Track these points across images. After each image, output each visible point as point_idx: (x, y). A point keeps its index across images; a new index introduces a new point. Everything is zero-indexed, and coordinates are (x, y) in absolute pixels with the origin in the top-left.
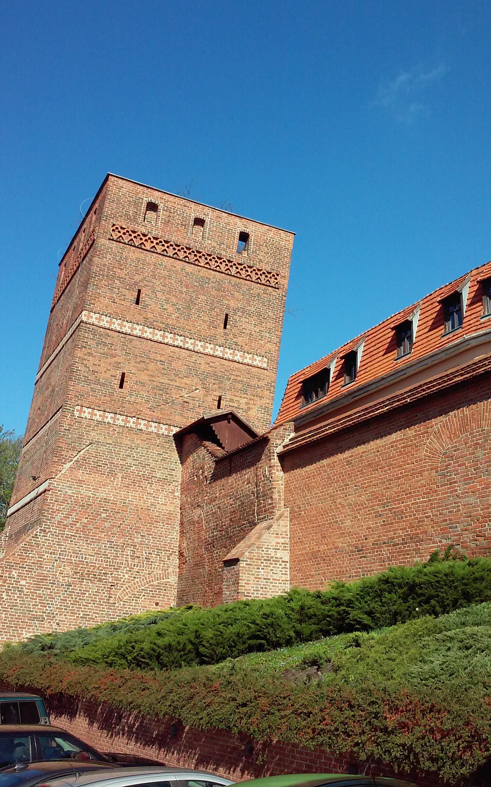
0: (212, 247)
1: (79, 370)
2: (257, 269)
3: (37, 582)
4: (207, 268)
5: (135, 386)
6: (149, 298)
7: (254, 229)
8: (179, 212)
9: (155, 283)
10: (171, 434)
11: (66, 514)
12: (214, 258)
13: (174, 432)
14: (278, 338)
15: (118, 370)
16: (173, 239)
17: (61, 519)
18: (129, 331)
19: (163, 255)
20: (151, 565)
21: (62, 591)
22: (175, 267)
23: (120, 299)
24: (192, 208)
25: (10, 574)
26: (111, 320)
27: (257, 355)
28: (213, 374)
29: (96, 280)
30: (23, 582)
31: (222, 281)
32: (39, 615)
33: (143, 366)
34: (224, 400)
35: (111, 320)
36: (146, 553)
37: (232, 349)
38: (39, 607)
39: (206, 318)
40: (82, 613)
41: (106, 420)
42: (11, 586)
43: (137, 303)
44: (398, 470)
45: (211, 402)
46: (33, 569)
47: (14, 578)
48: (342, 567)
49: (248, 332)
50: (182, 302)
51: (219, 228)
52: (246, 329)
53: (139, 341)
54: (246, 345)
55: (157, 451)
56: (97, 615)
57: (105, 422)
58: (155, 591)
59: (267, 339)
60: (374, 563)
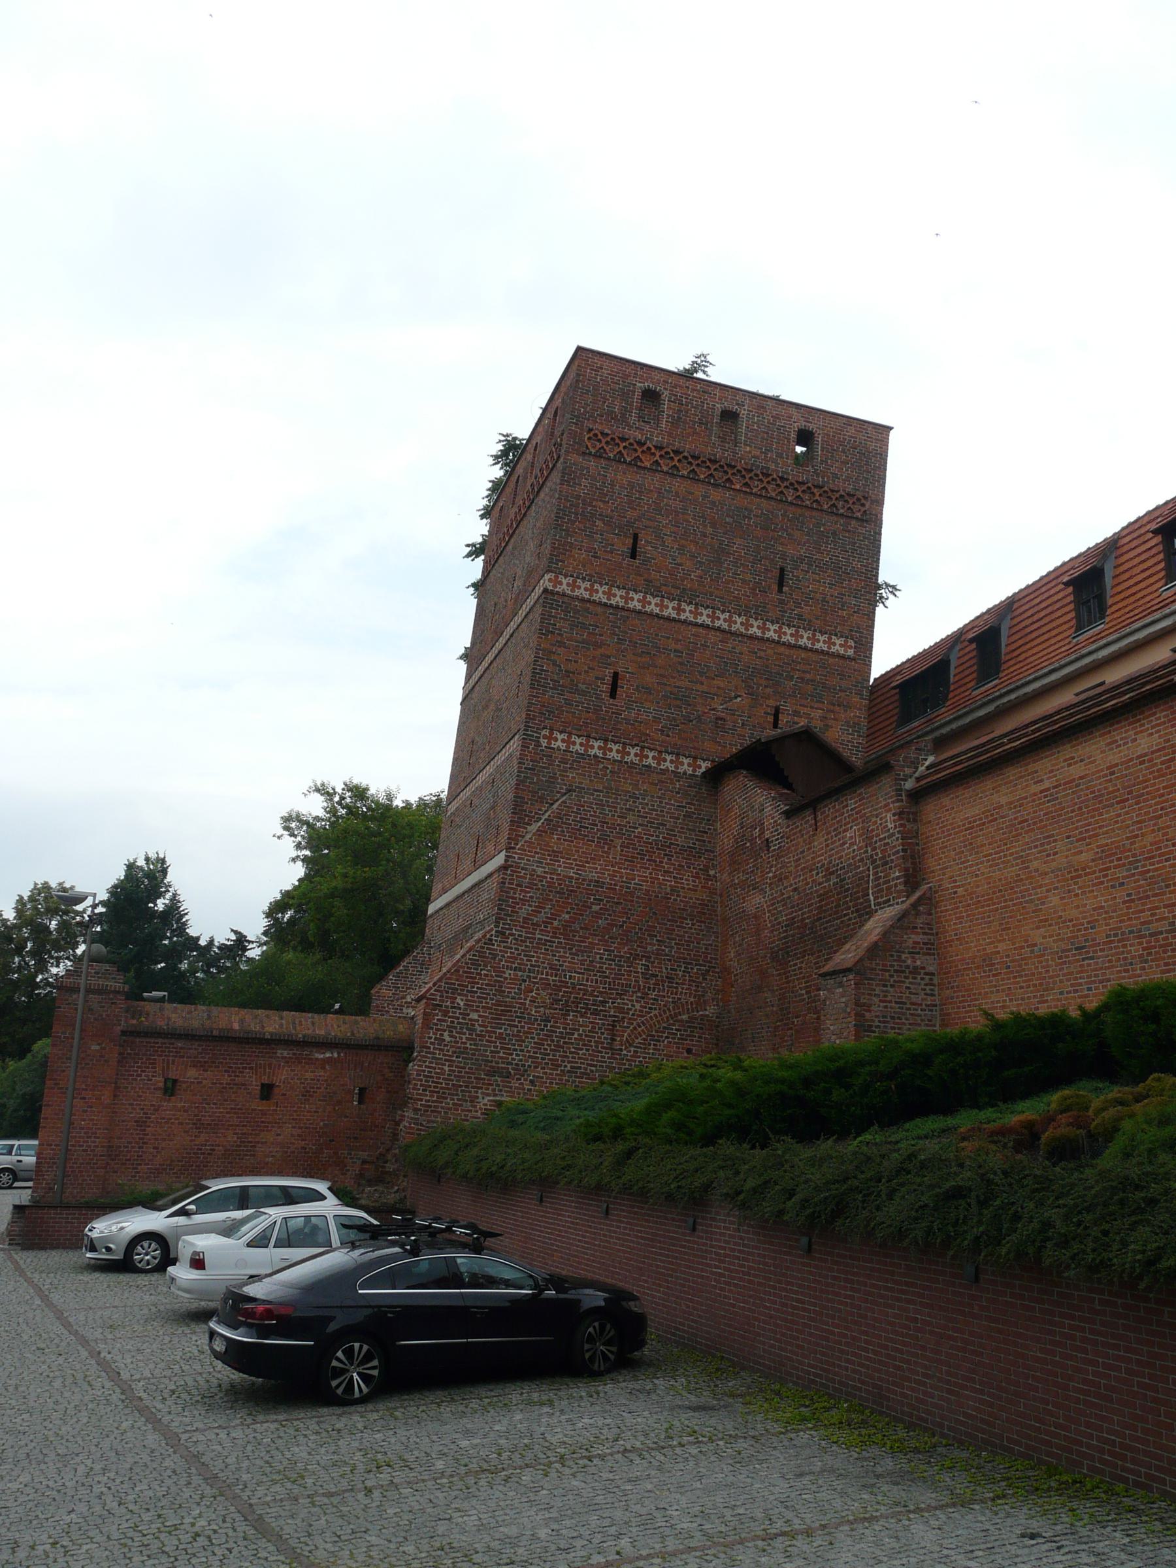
1: (545, 671)
3: (496, 1014)
4: (746, 492)
10: (699, 772)
11: (536, 907)
12: (757, 475)
13: (703, 770)
16: (688, 447)
17: (528, 914)
18: (621, 603)
19: (672, 475)
20: (676, 988)
21: (536, 1029)
22: (693, 493)
23: (606, 551)
25: (452, 1003)
26: (592, 586)
27: (836, 635)
30: (474, 1016)
31: (772, 513)
32: (502, 1068)
35: (592, 586)
36: (667, 969)
37: (794, 626)
38: (501, 1055)
39: (749, 577)
40: (569, 1065)
41: (592, 752)
42: (456, 1021)
43: (633, 555)
44: (1156, 804)
45: (762, 717)
46: (489, 994)
47: (460, 1009)
48: (1044, 978)
54: (817, 619)
55: (675, 801)
56: (593, 1068)
57: (590, 756)
58: (685, 1031)
60: (1112, 967)
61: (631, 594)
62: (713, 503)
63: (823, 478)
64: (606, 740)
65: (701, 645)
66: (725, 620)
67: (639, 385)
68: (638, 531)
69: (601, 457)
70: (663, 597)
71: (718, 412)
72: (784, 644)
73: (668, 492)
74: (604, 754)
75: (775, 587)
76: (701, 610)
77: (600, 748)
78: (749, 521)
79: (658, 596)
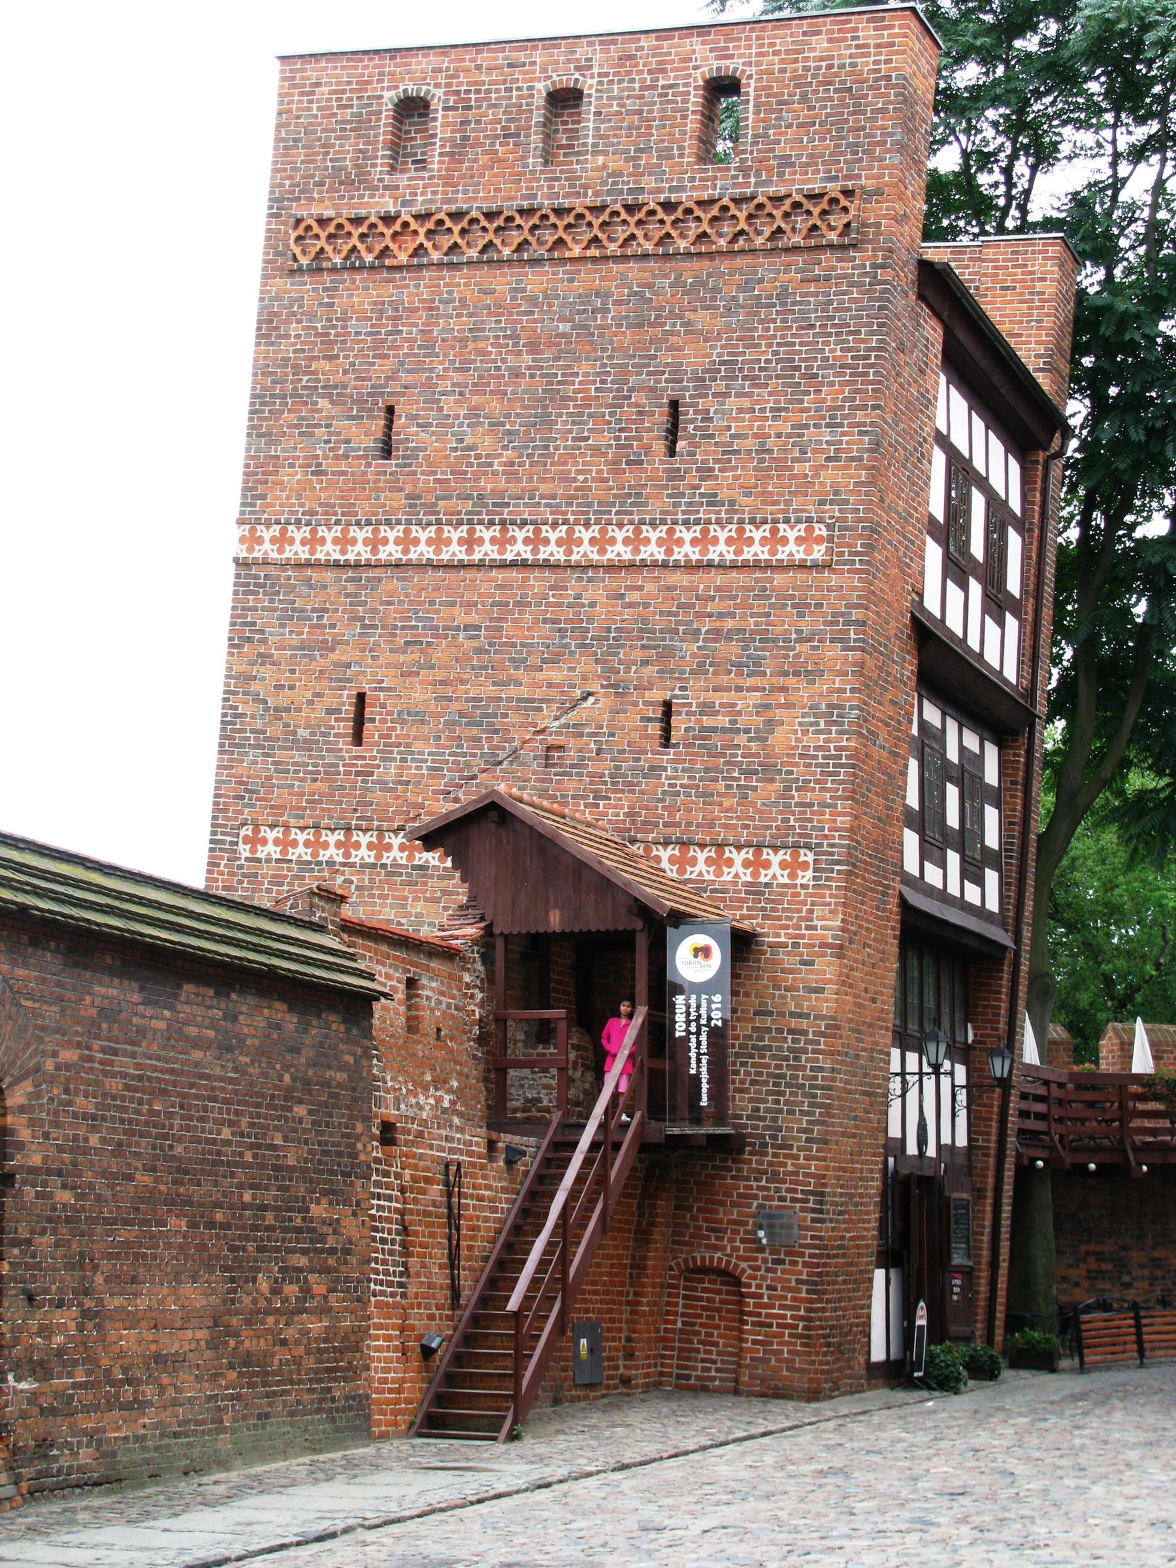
0: (609, 176)
1: (243, 715)
2: (770, 199)
4: (594, 259)
5: (394, 729)
6: (419, 425)
7: (754, 51)
8: (493, 96)
9: (432, 370)
14: (866, 432)
15: (344, 688)
18: (366, 555)
19: (452, 266)
22: (493, 292)
23: (336, 457)
24: (533, 63)
26: (314, 532)
27: (787, 521)
28: (640, 630)
29: (265, 419)
31: (650, 286)
33: (416, 656)
34: (679, 713)
37: (697, 522)
41: (324, 855)
43: (387, 451)
45: (635, 729)
49: (751, 443)
50: (524, 407)
51: (628, 97)
52: (745, 437)
53: (398, 579)
54: (747, 495)
57: (319, 863)
59: (822, 451)
61: (385, 532)
62: (533, 300)
63: (758, 174)
64: (348, 829)
65: (516, 604)
66: (559, 542)
67: (388, 95)
68: (392, 400)
69: (320, 270)
70: (439, 522)
71: (539, 100)
72: (676, 566)
73: (447, 302)
74: (347, 855)
75: (659, 446)
76: (513, 531)
77: (339, 845)
78: (604, 318)
79: (429, 524)
